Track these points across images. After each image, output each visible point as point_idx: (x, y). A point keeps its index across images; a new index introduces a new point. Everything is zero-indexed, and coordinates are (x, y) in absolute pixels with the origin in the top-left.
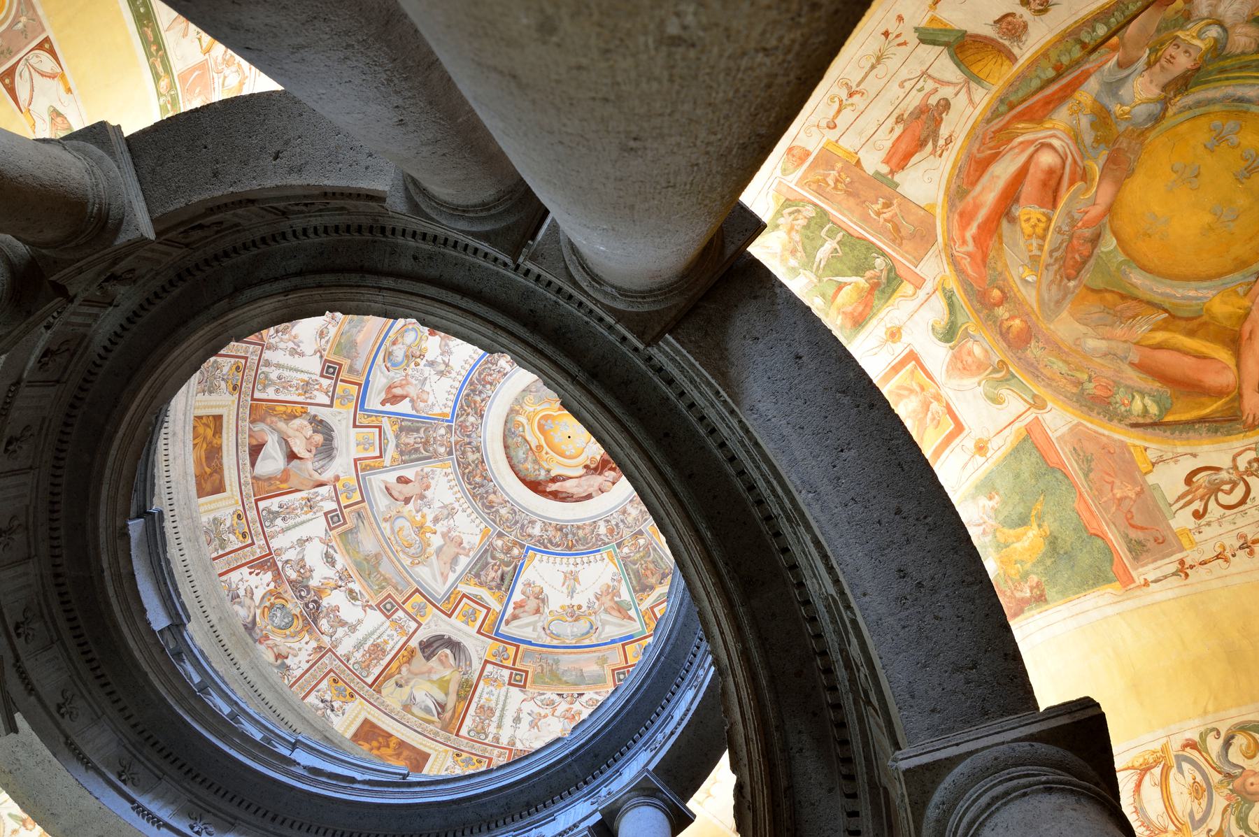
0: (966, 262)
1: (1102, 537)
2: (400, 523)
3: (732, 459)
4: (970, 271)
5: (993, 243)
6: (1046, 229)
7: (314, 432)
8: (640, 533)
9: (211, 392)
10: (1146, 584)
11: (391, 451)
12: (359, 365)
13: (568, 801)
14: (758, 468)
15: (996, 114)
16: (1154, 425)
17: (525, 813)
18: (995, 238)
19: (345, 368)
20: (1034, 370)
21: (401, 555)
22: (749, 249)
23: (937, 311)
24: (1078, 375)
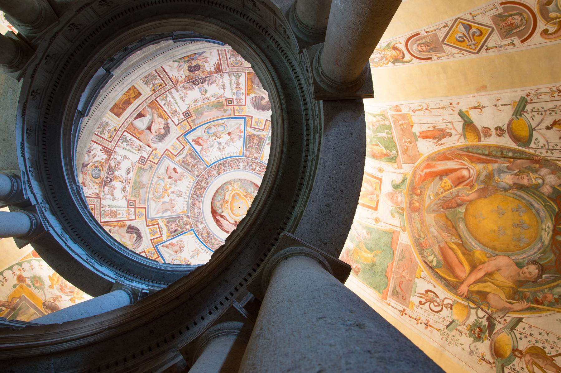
0: (418, 176)
1: (388, 280)
2: (161, 182)
3: (306, 161)
4: (417, 179)
5: (430, 179)
6: (448, 190)
7: (163, 128)
9: (145, 84)
10: (389, 304)
11: (180, 158)
12: (198, 122)
13: (141, 281)
14: (311, 168)
15: (462, 149)
16: (431, 267)
17: (125, 272)
18: (432, 178)
19: (192, 118)
20: (410, 220)
21: (151, 192)
22: (364, 100)
23: (399, 179)
24: (422, 234)
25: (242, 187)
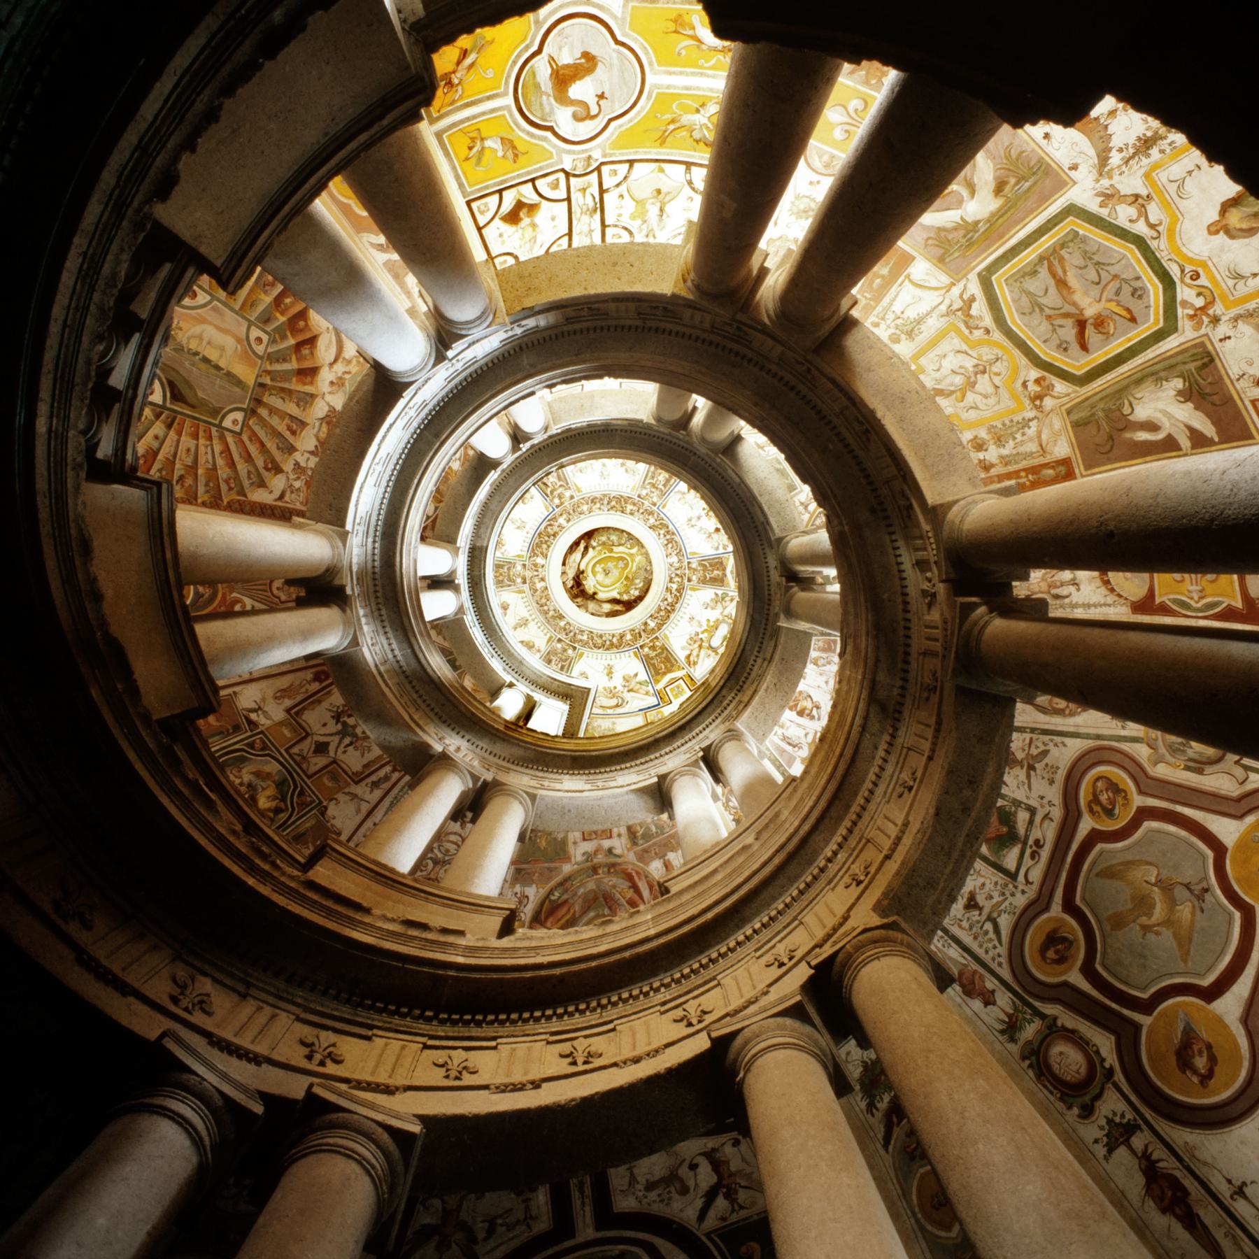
8: (524, 582)
23: (618, 851)
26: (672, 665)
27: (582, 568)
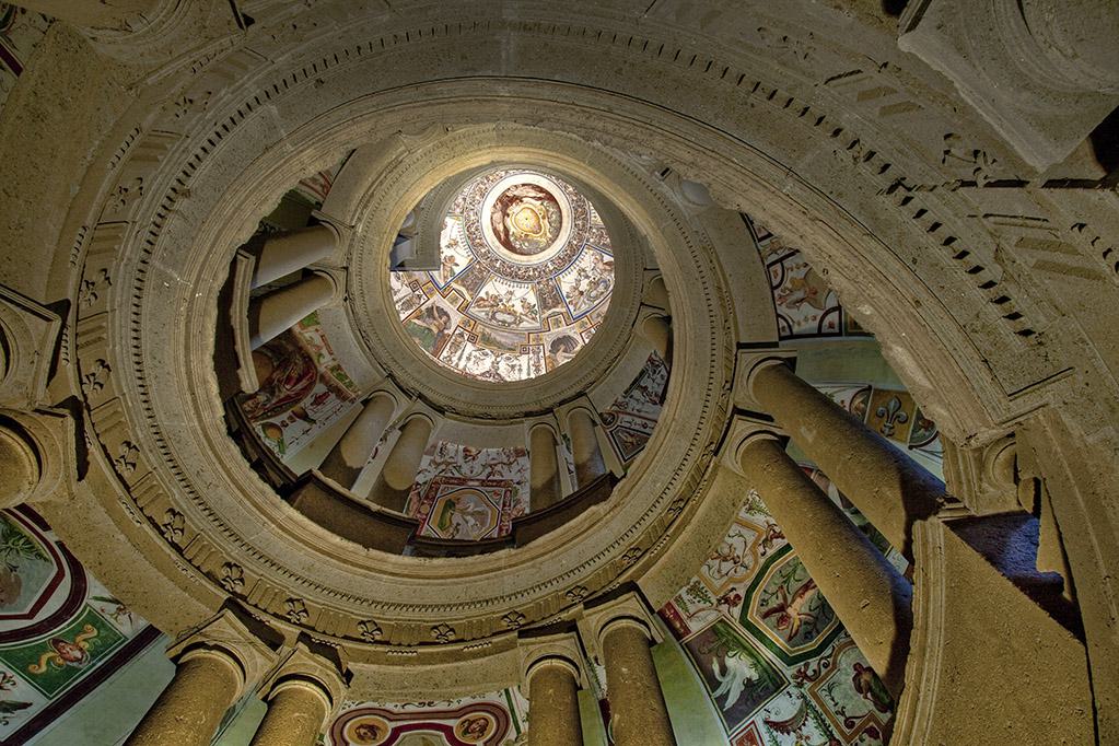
25: (537, 243)
26: (472, 290)
27: (525, 200)
